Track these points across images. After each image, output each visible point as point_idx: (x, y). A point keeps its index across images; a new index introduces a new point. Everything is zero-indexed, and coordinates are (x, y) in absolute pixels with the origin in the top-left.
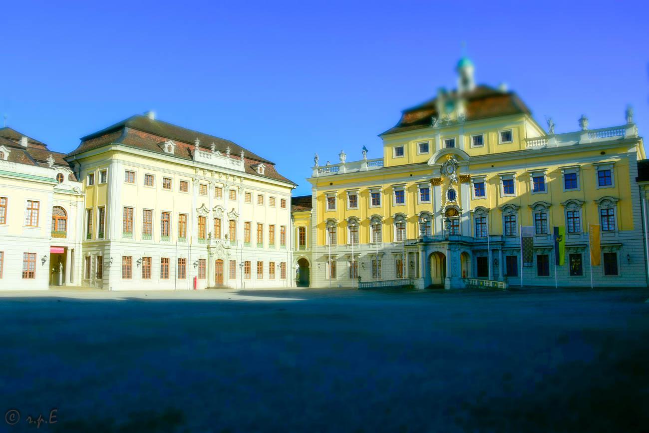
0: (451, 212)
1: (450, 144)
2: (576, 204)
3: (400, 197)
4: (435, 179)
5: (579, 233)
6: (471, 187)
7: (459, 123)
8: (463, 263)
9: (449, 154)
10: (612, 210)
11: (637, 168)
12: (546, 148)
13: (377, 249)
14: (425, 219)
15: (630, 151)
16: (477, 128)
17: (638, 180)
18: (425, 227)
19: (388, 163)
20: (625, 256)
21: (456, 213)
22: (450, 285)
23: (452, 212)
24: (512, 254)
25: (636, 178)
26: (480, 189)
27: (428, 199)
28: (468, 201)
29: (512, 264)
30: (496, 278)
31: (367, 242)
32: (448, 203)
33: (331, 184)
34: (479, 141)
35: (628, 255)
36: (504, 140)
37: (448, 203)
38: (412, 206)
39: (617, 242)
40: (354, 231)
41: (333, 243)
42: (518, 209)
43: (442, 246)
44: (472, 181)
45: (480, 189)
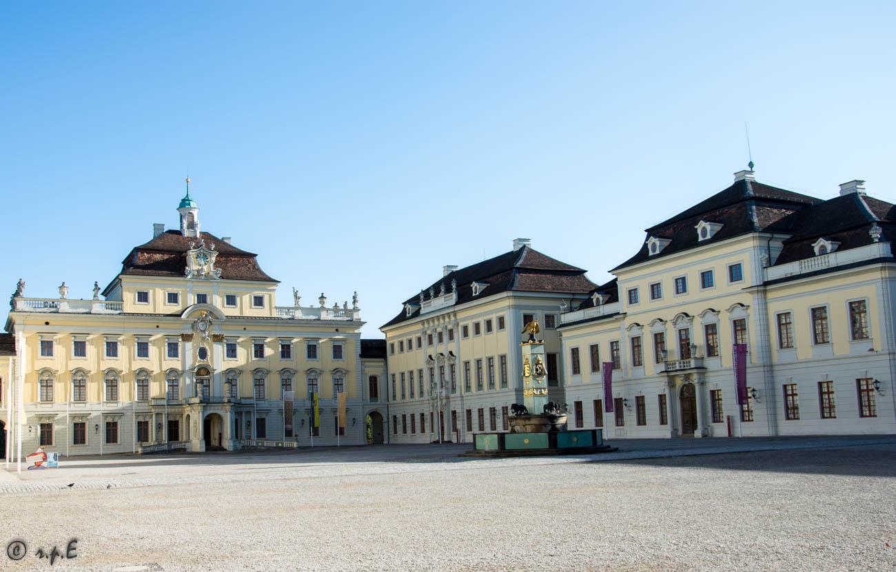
0: (202, 371)
1: (202, 298)
2: (342, 372)
3: (143, 350)
4: (186, 335)
6: (223, 347)
12: (293, 319)
13: (112, 407)
14: (173, 376)
15: (356, 331)
16: (231, 287)
17: (362, 356)
18: (173, 385)
21: (208, 373)
23: (203, 372)
26: (232, 352)
27: (176, 355)
28: (219, 361)
29: (261, 423)
31: (32, 400)
32: (199, 361)
33: (47, 323)
35: (354, 419)
37: (199, 361)
38: (156, 361)
40: (112, 386)
42: (268, 374)
43: (220, 408)
45: (232, 352)
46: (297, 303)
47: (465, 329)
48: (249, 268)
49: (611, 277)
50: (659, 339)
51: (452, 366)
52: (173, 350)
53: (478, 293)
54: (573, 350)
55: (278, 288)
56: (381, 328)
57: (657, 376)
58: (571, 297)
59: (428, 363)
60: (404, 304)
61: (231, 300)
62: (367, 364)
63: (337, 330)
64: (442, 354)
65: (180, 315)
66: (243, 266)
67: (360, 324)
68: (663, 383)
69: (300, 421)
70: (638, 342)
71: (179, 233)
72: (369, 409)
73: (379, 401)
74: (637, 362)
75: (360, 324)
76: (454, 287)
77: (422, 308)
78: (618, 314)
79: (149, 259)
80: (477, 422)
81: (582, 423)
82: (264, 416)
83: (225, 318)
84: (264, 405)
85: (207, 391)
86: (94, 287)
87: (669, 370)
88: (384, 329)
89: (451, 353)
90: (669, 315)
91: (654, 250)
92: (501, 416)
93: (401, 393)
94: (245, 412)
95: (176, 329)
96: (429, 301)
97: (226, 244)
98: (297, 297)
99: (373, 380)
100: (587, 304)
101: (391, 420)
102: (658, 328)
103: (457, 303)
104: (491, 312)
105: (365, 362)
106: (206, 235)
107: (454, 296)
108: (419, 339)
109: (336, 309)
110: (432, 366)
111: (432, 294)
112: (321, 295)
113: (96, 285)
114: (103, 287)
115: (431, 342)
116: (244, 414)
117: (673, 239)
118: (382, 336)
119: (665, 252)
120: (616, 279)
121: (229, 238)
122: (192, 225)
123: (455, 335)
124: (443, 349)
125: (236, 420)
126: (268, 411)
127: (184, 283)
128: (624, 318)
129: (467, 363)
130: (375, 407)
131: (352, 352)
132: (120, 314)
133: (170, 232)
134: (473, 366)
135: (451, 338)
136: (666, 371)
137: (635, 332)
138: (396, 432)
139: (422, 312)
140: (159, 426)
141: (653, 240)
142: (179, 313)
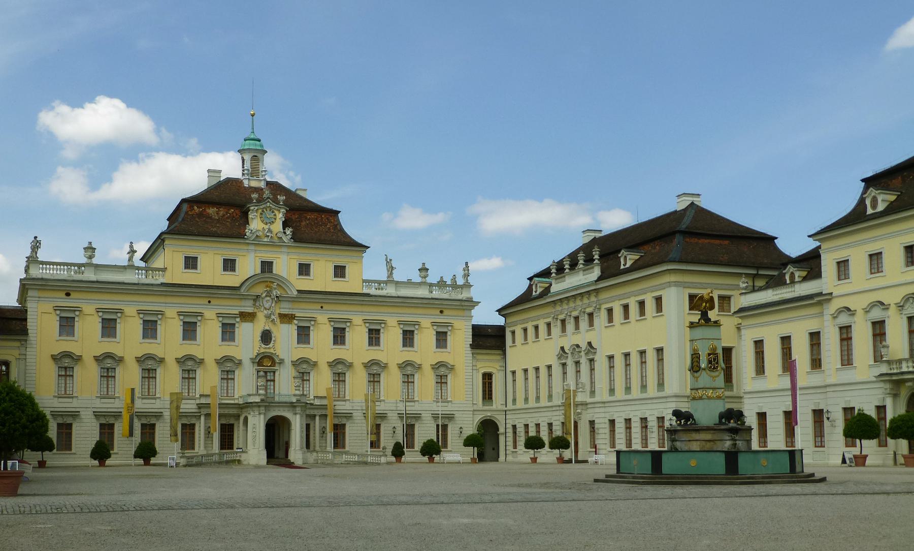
1: (267, 266)
7: (285, 242)
8: (835, 432)
16: (306, 254)
21: (274, 363)
22: (303, 458)
26: (304, 335)
29: (339, 432)
30: (324, 450)
32: (263, 349)
34: (304, 269)
35: (461, 428)
36: (336, 276)
44: (295, 322)
45: (304, 335)
46: (390, 274)
47: (610, 311)
49: (812, 244)
50: (879, 330)
52: (228, 332)
53: (628, 266)
54: (756, 342)
55: (367, 255)
56: (497, 311)
57: (875, 379)
58: (754, 272)
59: (560, 357)
60: (530, 279)
62: (479, 357)
63: (441, 312)
64: (578, 346)
66: (321, 225)
67: (470, 304)
68: (884, 390)
69: (391, 428)
70: (847, 333)
72: (478, 418)
74: (847, 360)
75: (470, 304)
76: (596, 257)
77: (553, 285)
78: (821, 294)
79: (200, 215)
80: (623, 436)
81: (765, 442)
82: (344, 421)
83: (295, 293)
84: (342, 407)
85: (272, 387)
86: (128, 249)
87: (892, 372)
89: (590, 344)
90: (893, 297)
91: (874, 206)
92: (655, 429)
93: (524, 397)
94: (321, 416)
95: (233, 307)
96: (563, 275)
97: (301, 198)
98: (391, 269)
99: (488, 378)
100: (777, 282)
101: (510, 430)
102: (877, 314)
103: (600, 279)
104: (644, 291)
107: (596, 272)
108: (549, 325)
109: (441, 284)
110: (562, 362)
111: (567, 266)
112: (420, 266)
113: (131, 247)
114: (142, 248)
115: (564, 329)
116: (317, 418)
117: (901, 193)
118: (500, 321)
119: (891, 209)
120: (819, 247)
121: (305, 190)
123: (596, 321)
124: (581, 339)
125: (308, 426)
126: (349, 416)
127: (245, 247)
128: (830, 299)
129: (611, 357)
131: (461, 338)
132: (163, 284)
133: (229, 181)
134: (619, 362)
135: (591, 324)
136: (887, 374)
137: (844, 320)
138: (515, 447)
139: (555, 288)
140: (208, 433)
141: (872, 192)
142: (238, 285)
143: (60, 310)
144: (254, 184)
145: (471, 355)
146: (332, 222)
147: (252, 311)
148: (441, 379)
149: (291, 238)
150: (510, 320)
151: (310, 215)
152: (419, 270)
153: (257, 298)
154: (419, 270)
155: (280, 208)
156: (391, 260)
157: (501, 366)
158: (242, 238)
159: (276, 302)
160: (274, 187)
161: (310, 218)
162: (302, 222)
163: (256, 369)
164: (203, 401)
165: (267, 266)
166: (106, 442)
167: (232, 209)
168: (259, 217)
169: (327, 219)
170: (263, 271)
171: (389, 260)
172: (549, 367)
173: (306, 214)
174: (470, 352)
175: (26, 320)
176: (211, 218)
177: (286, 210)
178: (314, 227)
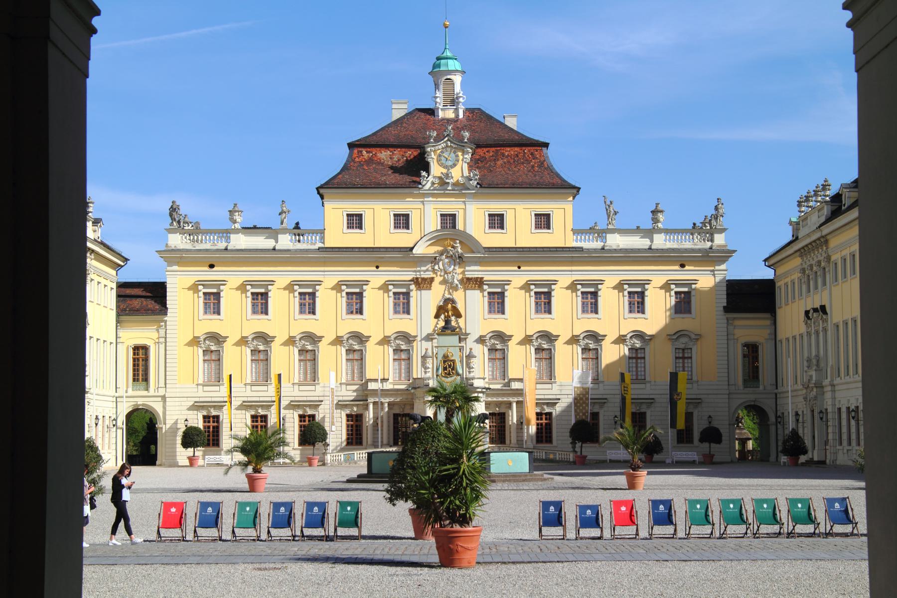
1: (449, 220)
5: (644, 381)
9: (451, 239)
10: (689, 351)
11: (725, 293)
17: (727, 309)
19: (332, 241)
20: (706, 418)
24: (638, 410)
25: (724, 307)
26: (497, 302)
33: (212, 266)
35: (710, 417)
36: (538, 226)
39: (694, 397)
41: (215, 378)
45: (497, 302)
48: (533, 167)
51: (825, 330)
52: (403, 304)
56: (765, 260)
59: (806, 324)
61: (497, 221)
62: (737, 323)
64: (815, 310)
65: (412, 249)
66: (523, 163)
69: (612, 418)
71: (431, 112)
73: (761, 387)
79: (370, 161)
88: (772, 261)
94: (518, 402)
98: (610, 214)
105: (734, 319)
106: (476, 115)
107: (826, 211)
112: (653, 208)
116: (514, 405)
118: (767, 274)
122: (453, 102)
130: (752, 397)
132: (319, 248)
142: (412, 246)
143: (203, 285)
144: (450, 114)
145: (726, 321)
146: (537, 158)
147: (429, 276)
148: (683, 353)
149: (478, 183)
150: (781, 270)
151: (509, 151)
152: (651, 212)
153: (434, 260)
154: (651, 212)
155: (463, 146)
156: (611, 203)
157: (769, 334)
158: (415, 187)
159: (459, 264)
160: (472, 116)
161: (508, 155)
162: (498, 160)
163: (435, 347)
164: (372, 386)
165: (449, 220)
166: (94, 438)
167: (409, 151)
168: (435, 161)
169: (532, 154)
170: (444, 226)
171: (608, 203)
172: (801, 336)
173: (503, 150)
174: (724, 317)
175: (166, 297)
176: (382, 164)
177: (471, 149)
178: (513, 167)
